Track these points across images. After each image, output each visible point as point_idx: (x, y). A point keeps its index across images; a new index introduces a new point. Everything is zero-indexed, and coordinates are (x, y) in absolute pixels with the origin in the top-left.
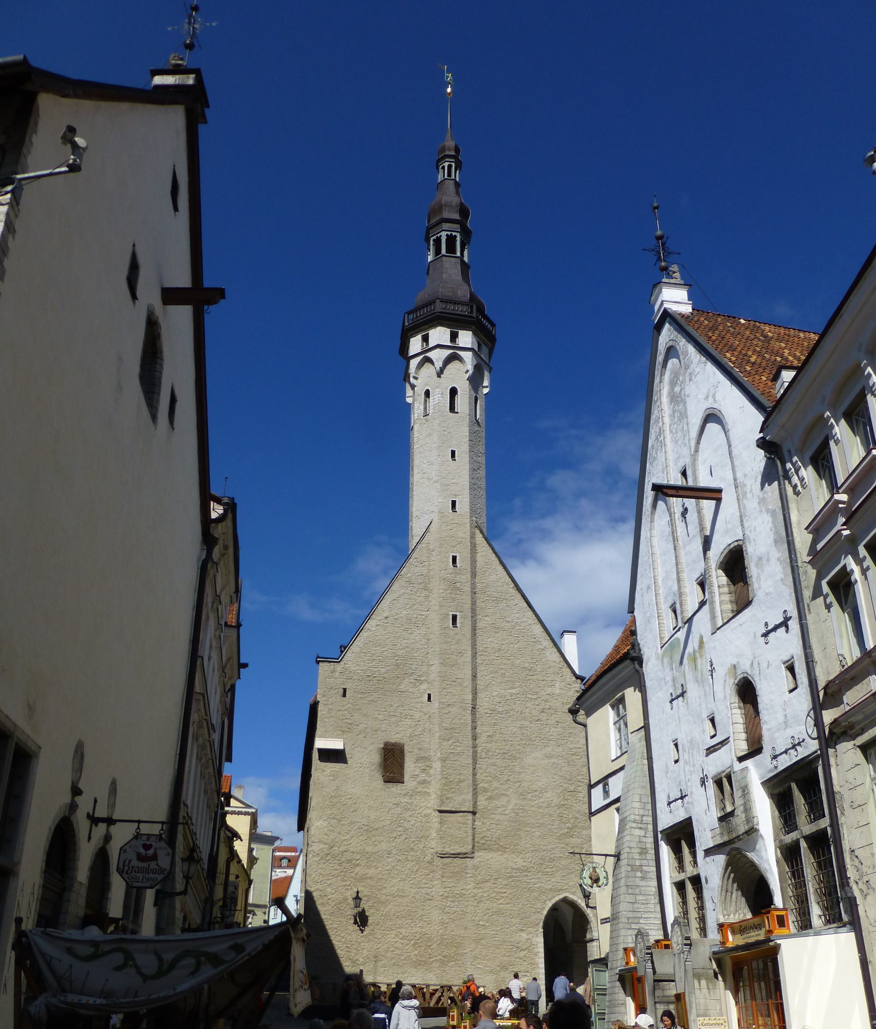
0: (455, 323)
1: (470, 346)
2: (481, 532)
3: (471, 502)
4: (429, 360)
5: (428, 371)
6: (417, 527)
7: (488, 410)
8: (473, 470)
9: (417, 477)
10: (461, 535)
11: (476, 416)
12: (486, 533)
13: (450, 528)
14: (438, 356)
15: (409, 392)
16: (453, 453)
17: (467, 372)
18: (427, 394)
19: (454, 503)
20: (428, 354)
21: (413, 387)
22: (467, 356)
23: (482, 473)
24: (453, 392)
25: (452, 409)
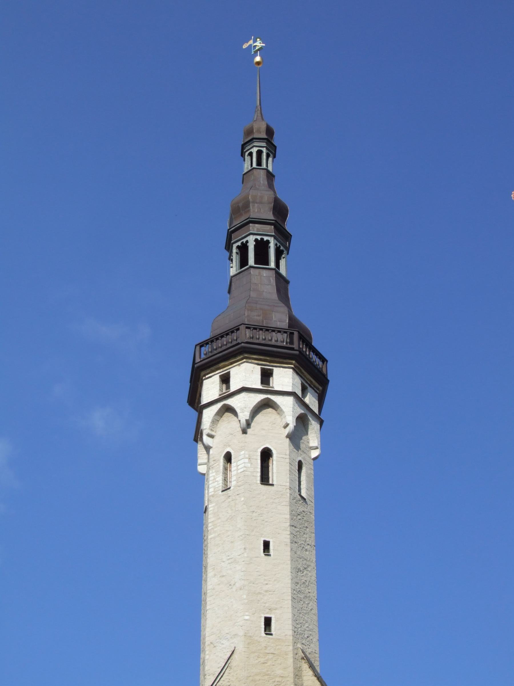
0: (269, 355)
1: (289, 389)
2: (311, 666)
3: (295, 620)
4: (229, 409)
5: (230, 425)
6: (212, 661)
7: (318, 482)
8: (297, 571)
9: (212, 582)
10: (279, 672)
11: (300, 490)
12: (318, 669)
13: (262, 660)
14: (242, 404)
15: (202, 456)
16: (266, 545)
17: (286, 426)
18: (228, 458)
19: (268, 622)
20: (230, 402)
21: (208, 449)
22: (287, 404)
23: (312, 575)
24: (266, 455)
25: (265, 479)
